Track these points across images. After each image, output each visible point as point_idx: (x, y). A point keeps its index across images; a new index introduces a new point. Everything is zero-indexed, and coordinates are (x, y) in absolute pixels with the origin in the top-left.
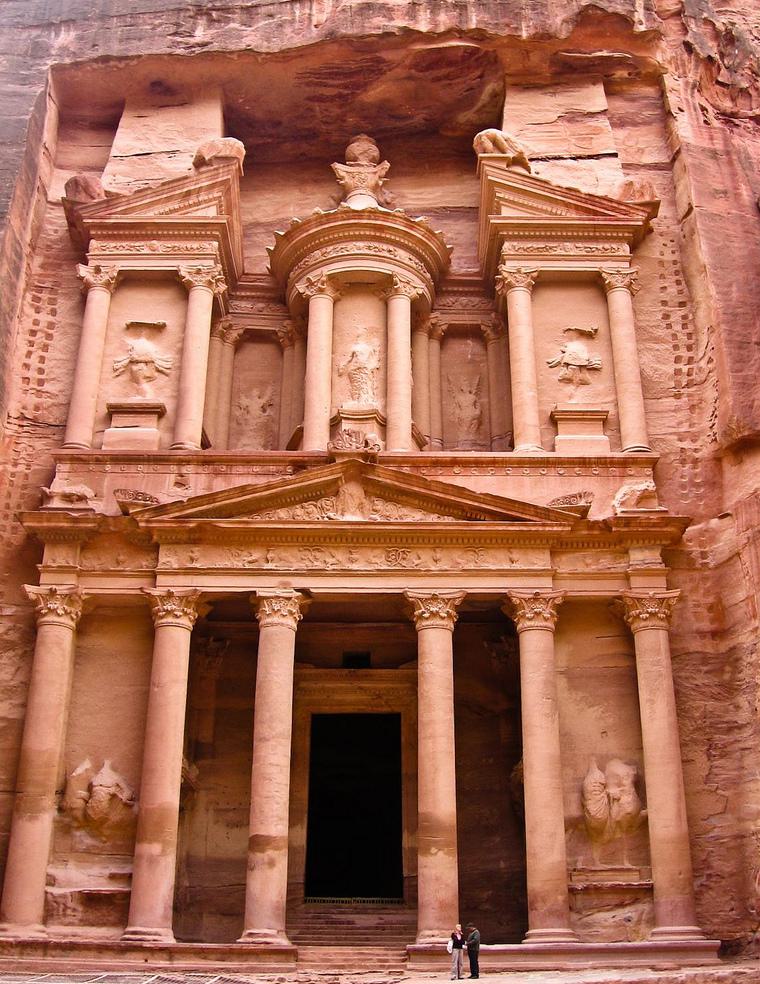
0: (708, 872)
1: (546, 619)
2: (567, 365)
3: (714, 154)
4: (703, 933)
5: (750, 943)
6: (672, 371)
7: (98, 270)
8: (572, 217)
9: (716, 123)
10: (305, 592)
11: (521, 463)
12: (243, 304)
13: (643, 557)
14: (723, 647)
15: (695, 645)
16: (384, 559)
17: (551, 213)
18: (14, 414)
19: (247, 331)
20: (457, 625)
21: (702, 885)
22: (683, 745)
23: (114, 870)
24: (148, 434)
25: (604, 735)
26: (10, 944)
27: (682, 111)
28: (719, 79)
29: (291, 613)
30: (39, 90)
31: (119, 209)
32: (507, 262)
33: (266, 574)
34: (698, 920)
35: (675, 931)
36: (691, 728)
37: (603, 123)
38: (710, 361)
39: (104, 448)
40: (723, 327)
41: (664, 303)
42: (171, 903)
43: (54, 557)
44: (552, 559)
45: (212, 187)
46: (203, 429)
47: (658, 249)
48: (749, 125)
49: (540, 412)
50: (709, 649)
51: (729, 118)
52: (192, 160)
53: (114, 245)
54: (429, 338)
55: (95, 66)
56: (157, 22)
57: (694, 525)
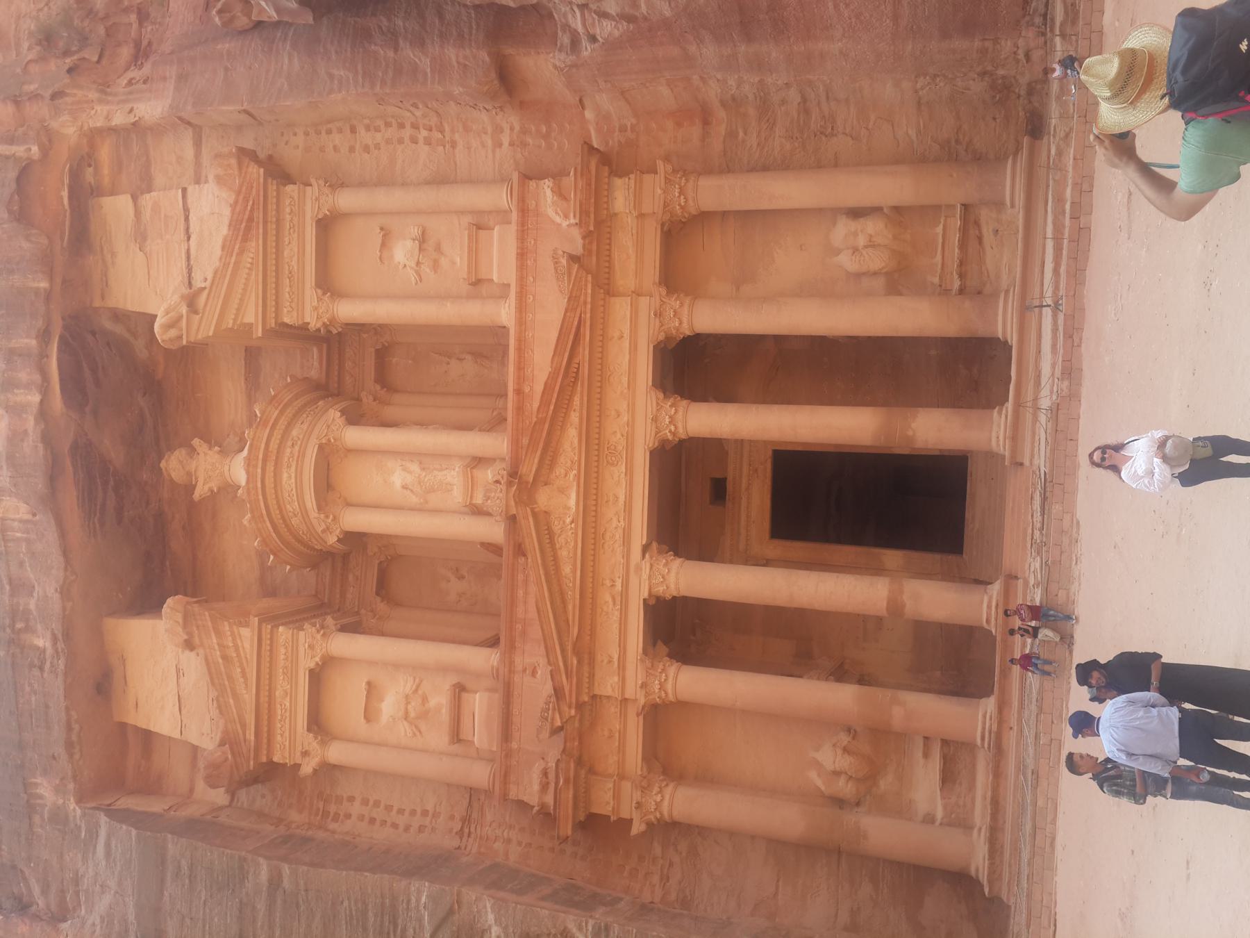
0: (953, 143)
1: (682, 305)
2: (418, 263)
3: (182, 78)
4: (1016, 154)
6: (427, 148)
7: (305, 754)
8: (255, 246)
9: (147, 69)
10: (645, 549)
11: (521, 322)
12: (349, 596)
13: (621, 196)
14: (722, 114)
17: (250, 269)
18: (456, 843)
19: (377, 594)
20: (683, 396)
22: (819, 166)
23: (920, 754)
24: (480, 705)
26: (992, 864)
27: (131, 111)
28: (95, 59)
29: (666, 565)
30: (103, 819)
31: (240, 731)
32: (307, 320)
34: (1001, 159)
35: (1011, 182)
37: (147, 200)
38: (415, 106)
39: (494, 749)
40: (378, 89)
41: (352, 149)
42: (955, 699)
43: (603, 802)
44: (624, 295)
45: (219, 634)
46: (476, 645)
47: (293, 151)
48: (149, 29)
49: (469, 297)
50: (722, 129)
51: (141, 53)
52: (187, 652)
53: (279, 738)
54: (389, 404)
55: (77, 756)
56: (27, 689)
57: (590, 137)
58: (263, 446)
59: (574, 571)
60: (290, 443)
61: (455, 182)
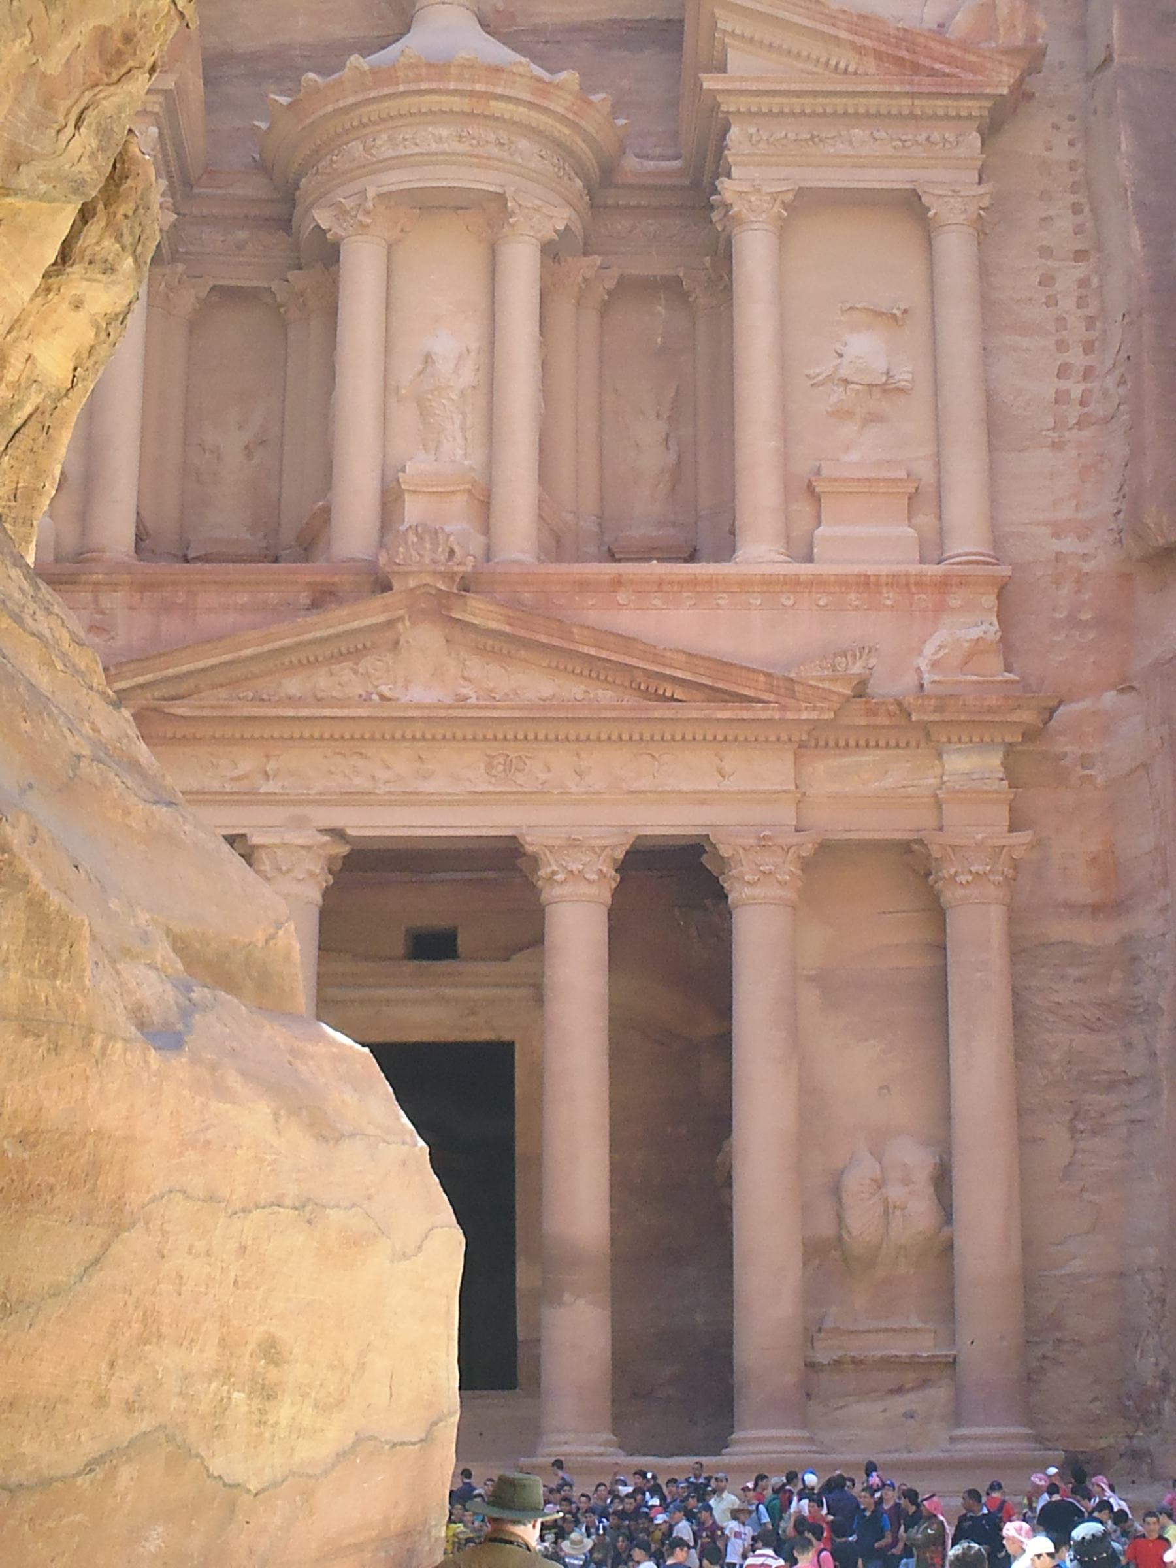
0: (1059, 1335)
2: (846, 382)
5: (1121, 1456)
10: (338, 834)
11: (745, 584)
13: (971, 765)
15: (1060, 929)
16: (483, 766)
20: (616, 893)
21: (1044, 1357)
22: (1021, 1113)
25: (885, 1091)
29: (311, 874)
32: (735, 172)
33: (264, 803)
34: (1029, 1414)
36: (1043, 1082)
38: (1121, 382)
41: (1046, 252)
58: (499, 90)
59: (291, 701)
60: (504, 137)
61: (991, 448)
